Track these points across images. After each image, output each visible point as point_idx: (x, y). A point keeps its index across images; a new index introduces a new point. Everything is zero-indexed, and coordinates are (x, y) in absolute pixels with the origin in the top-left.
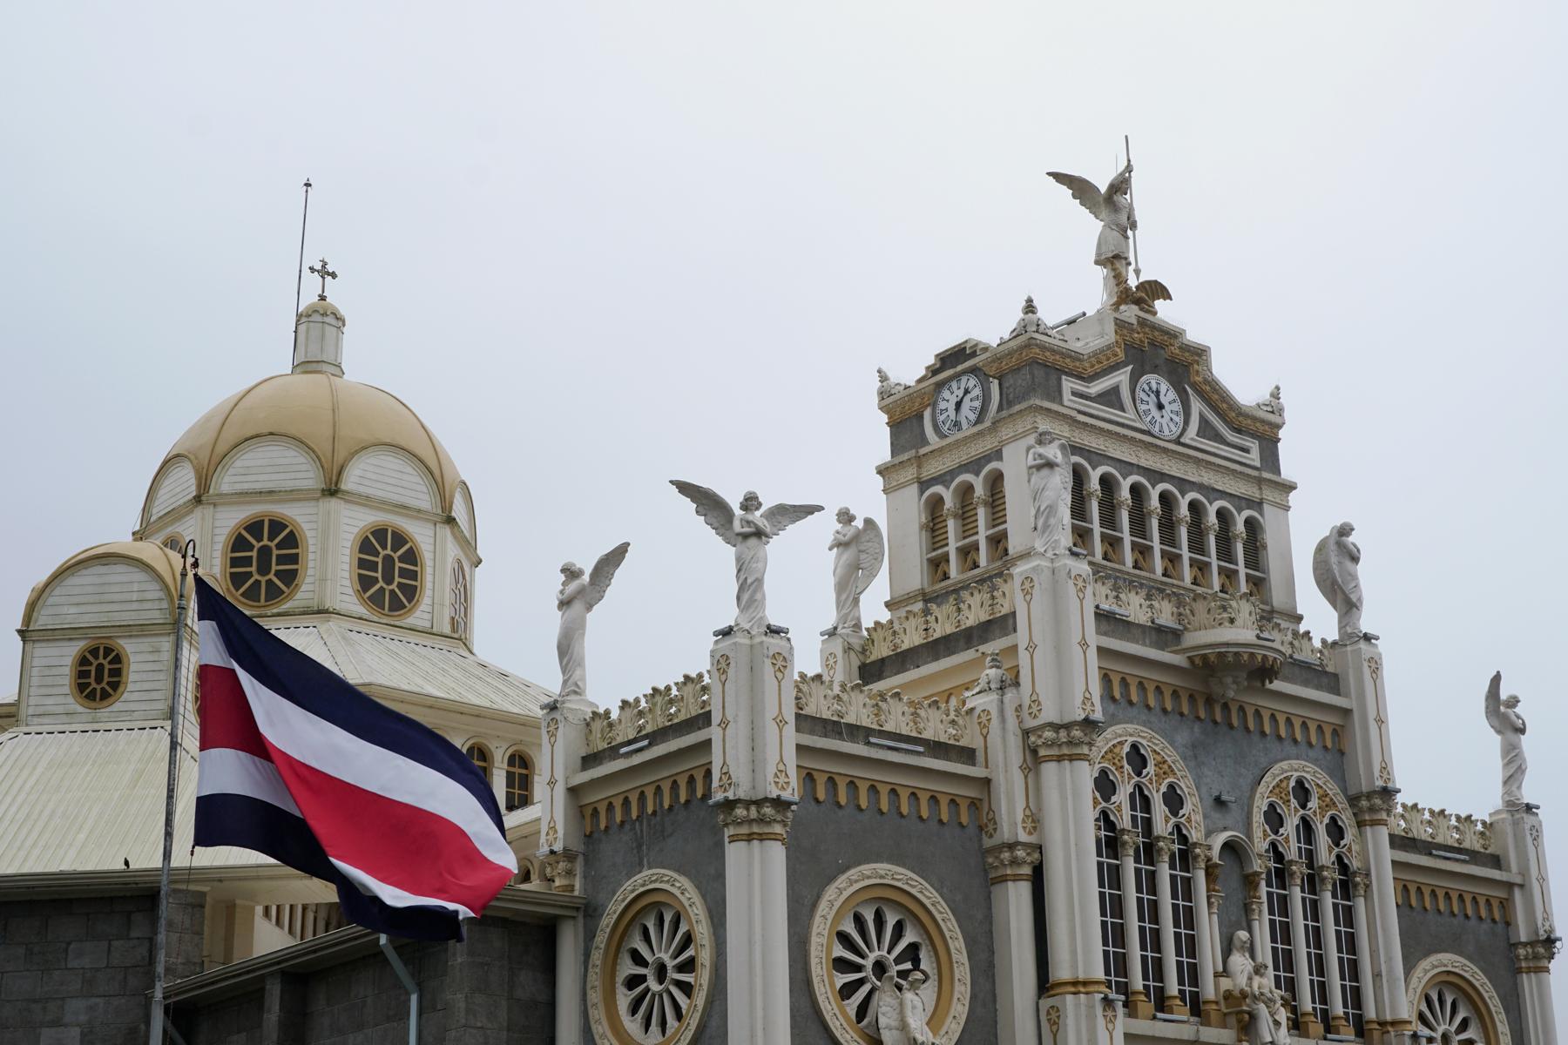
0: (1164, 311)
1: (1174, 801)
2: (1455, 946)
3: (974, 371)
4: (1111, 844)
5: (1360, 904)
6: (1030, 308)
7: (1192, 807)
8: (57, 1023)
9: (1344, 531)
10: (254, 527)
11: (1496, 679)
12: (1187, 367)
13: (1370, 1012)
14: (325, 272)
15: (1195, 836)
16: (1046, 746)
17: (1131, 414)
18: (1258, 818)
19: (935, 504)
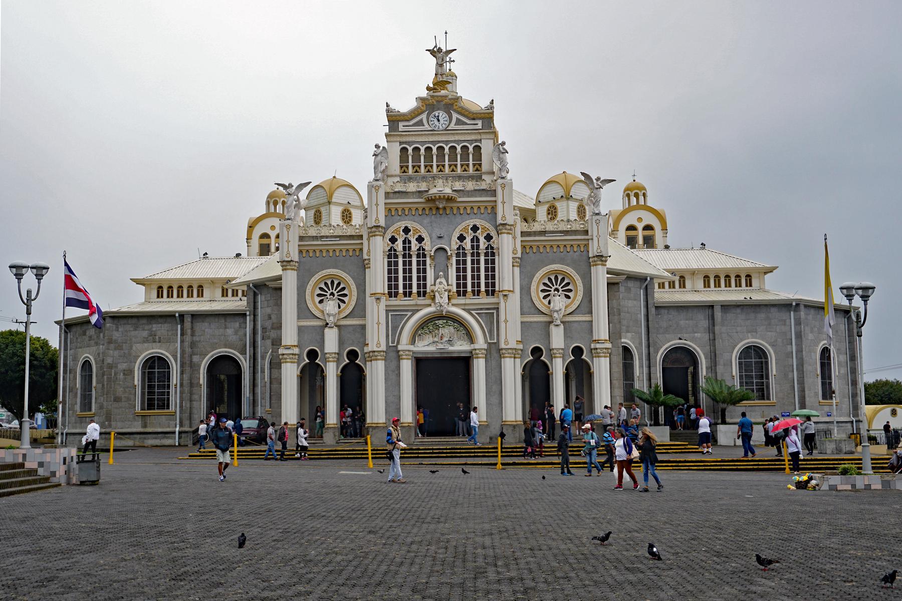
1: (420, 239)
2: (562, 261)
4: (391, 254)
5: (496, 258)
6: (388, 105)
7: (427, 240)
12: (452, 104)
13: (497, 289)
15: (426, 248)
16: (375, 230)
18: (455, 238)
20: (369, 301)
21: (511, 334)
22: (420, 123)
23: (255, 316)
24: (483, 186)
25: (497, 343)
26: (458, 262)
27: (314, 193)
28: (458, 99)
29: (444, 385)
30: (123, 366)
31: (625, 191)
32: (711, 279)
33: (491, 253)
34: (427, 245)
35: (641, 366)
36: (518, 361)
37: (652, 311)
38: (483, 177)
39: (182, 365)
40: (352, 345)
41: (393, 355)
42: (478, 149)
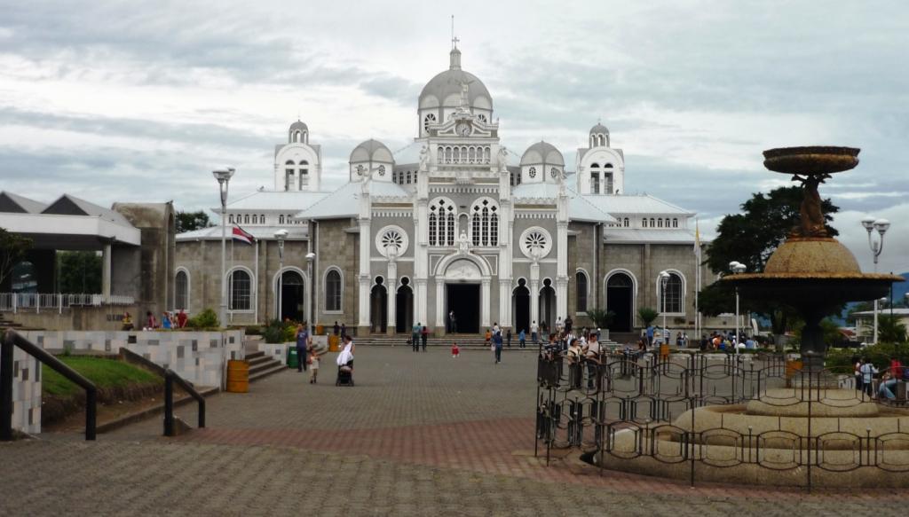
1: (450, 208)
4: (432, 218)
14: (455, 40)
17: (455, 134)
20: (417, 249)
21: (505, 271)
22: (451, 132)
24: (491, 176)
25: (498, 276)
26: (474, 224)
28: (464, 73)
29: (463, 300)
30: (214, 277)
31: (591, 132)
32: (649, 220)
33: (495, 218)
34: (454, 211)
35: (592, 287)
36: (510, 288)
37: (602, 247)
38: (491, 169)
39: (259, 277)
40: (404, 274)
41: (431, 282)
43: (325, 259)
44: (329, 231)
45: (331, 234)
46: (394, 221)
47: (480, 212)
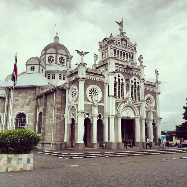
0: (125, 35)
3: (106, 40)
4: (115, 83)
6: (111, 34)
8: (28, 98)
9: (141, 56)
10: (50, 56)
11: (156, 70)
14: (57, 33)
19: (103, 53)
23: (9, 99)
27: (31, 60)
41: (116, 117)
42: (132, 55)
43: (16, 108)
44: (19, 93)
45: (20, 95)
46: (95, 82)
47: (133, 83)
